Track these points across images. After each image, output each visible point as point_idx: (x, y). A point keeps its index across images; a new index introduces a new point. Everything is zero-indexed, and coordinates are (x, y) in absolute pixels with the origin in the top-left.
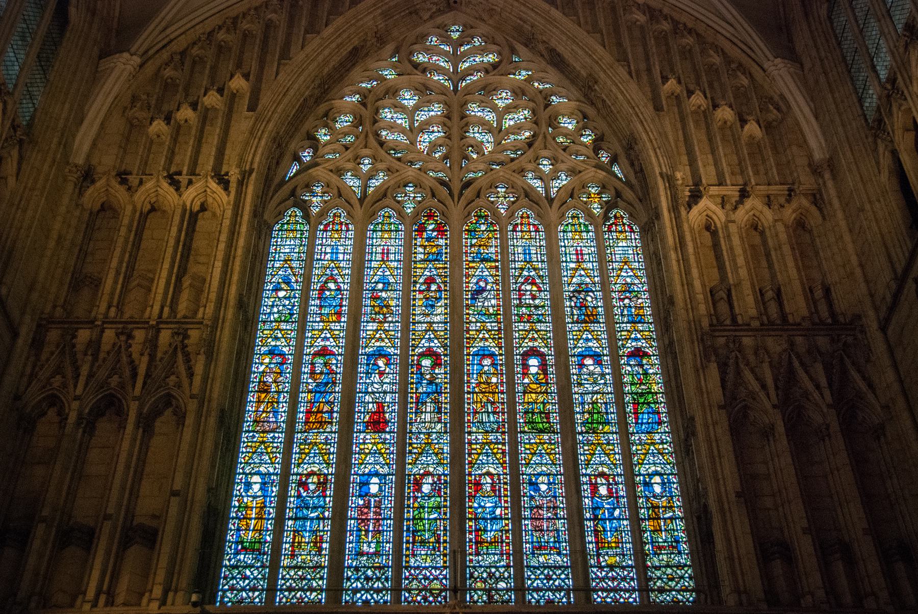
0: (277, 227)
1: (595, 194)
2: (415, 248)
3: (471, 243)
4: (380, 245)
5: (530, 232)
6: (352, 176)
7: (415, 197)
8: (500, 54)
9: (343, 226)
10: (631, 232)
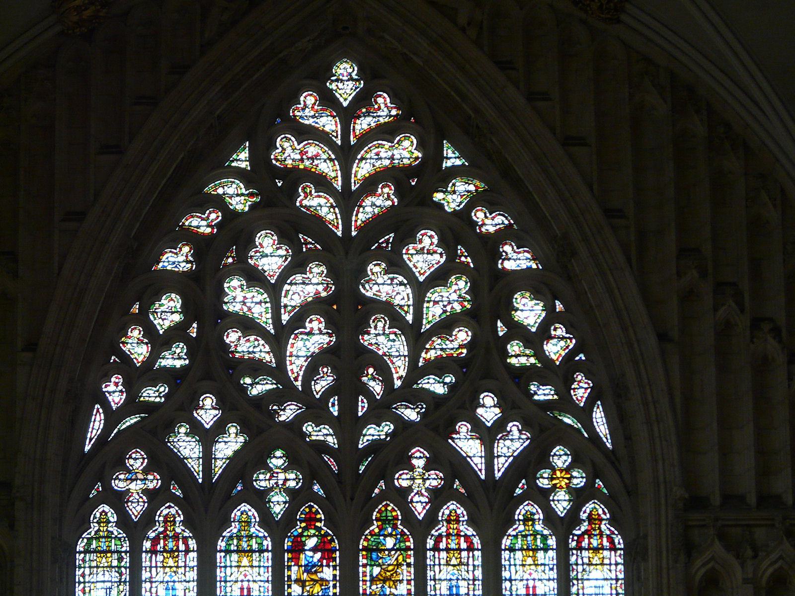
0: (80, 547)
1: (561, 471)
2: (289, 586)
3: (371, 575)
4: (236, 582)
5: (460, 550)
6: (187, 434)
7: (286, 480)
8: (420, 146)
9: (181, 542)
10: (610, 549)
